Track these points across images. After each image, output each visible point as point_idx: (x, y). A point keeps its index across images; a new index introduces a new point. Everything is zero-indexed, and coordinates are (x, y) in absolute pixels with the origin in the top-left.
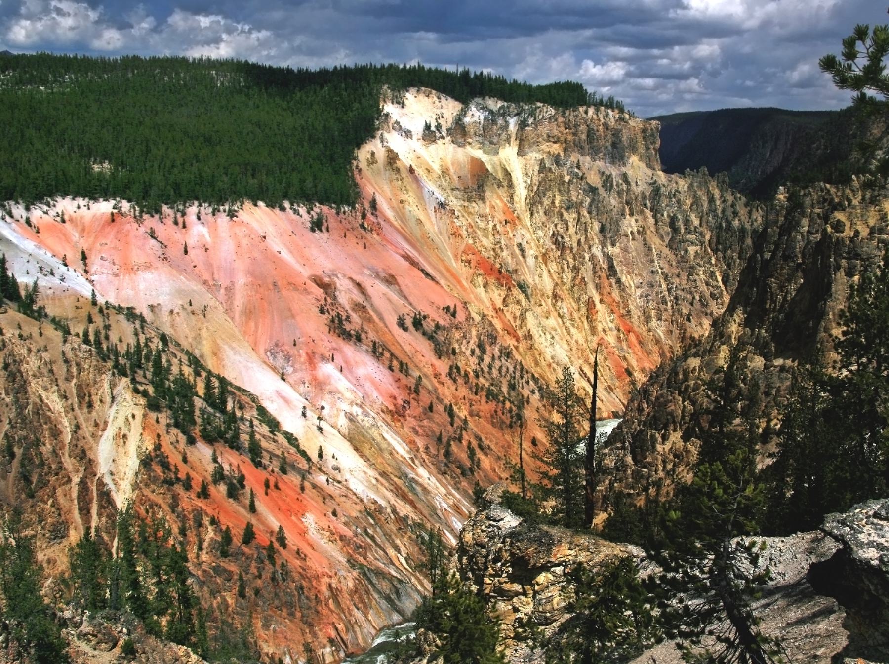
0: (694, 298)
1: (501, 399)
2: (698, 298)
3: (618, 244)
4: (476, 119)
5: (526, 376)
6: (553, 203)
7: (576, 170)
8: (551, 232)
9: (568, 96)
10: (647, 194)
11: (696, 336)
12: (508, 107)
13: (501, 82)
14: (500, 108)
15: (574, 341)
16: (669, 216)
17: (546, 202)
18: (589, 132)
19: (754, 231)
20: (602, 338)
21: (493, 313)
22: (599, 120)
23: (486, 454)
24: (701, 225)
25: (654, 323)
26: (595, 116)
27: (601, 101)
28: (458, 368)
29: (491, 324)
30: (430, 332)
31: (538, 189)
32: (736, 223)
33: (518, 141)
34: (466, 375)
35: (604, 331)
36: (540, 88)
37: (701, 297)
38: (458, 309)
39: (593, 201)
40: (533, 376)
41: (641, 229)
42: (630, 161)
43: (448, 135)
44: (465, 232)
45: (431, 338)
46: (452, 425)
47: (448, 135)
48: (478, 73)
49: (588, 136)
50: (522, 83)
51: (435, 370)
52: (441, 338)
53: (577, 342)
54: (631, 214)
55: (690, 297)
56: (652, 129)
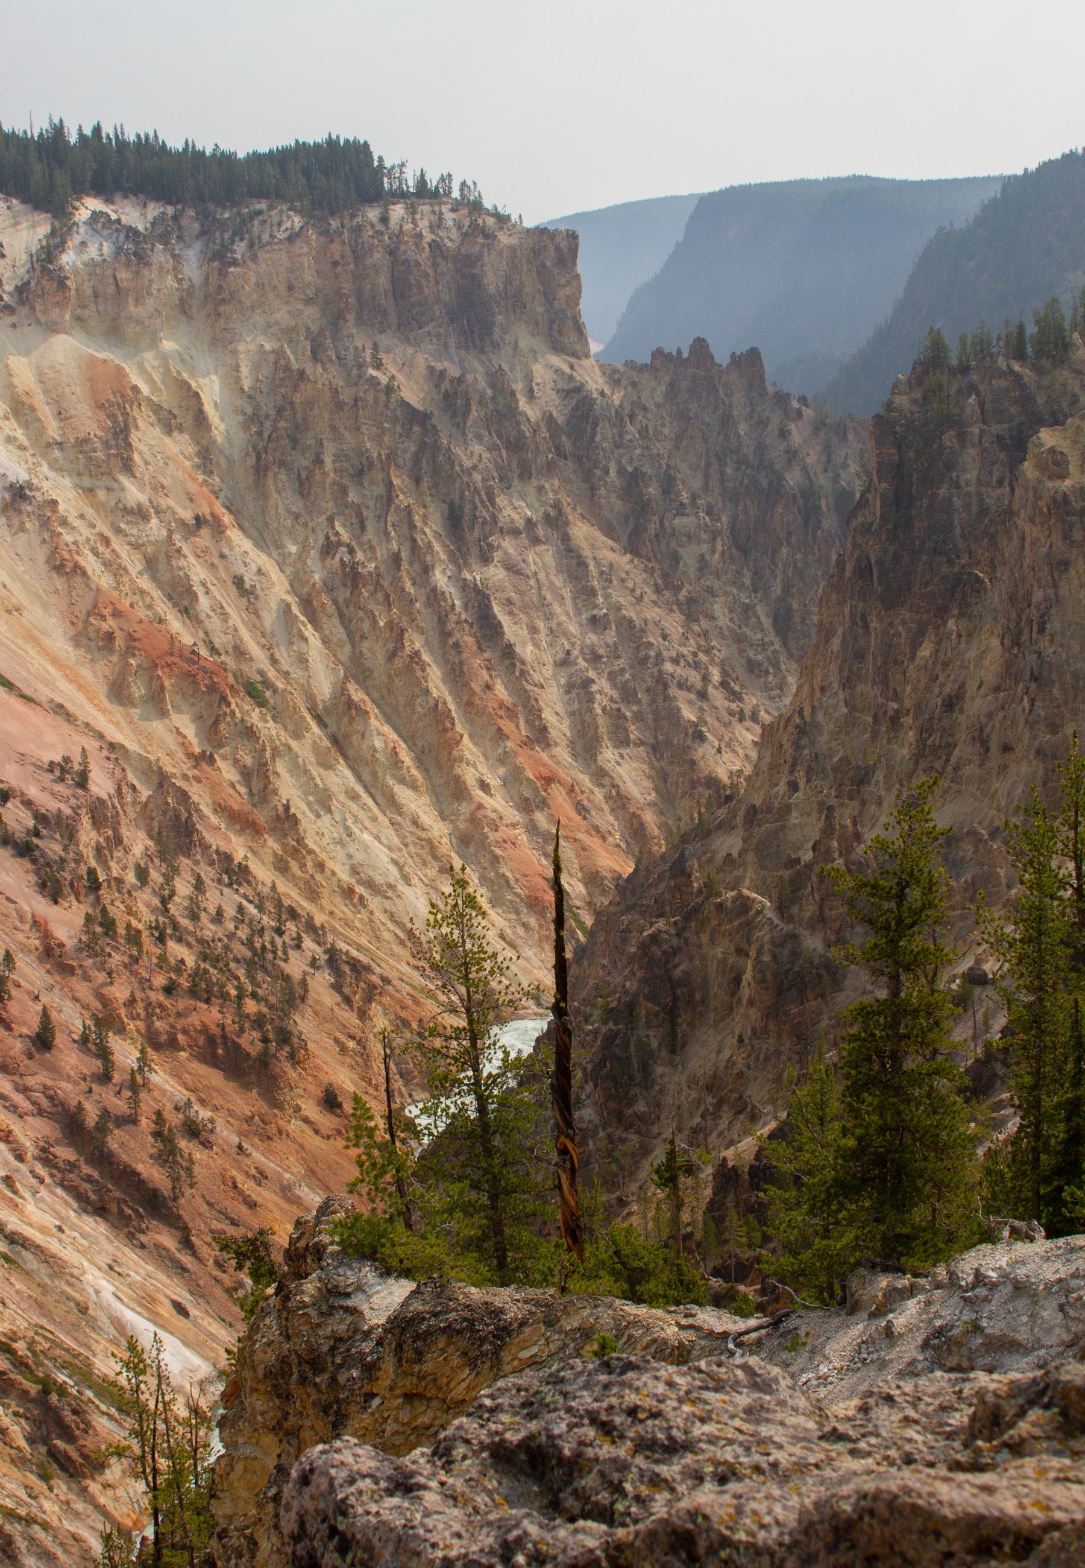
0: (706, 679)
1: (234, 992)
2: (716, 676)
3: (497, 556)
4: (93, 252)
5: (291, 927)
6: (319, 461)
7: (372, 372)
8: (321, 540)
9: (334, 177)
10: (561, 420)
11: (724, 777)
12: (175, 218)
13: (148, 150)
14: (153, 224)
15: (407, 824)
16: (622, 471)
17: (303, 461)
18: (393, 265)
19: (843, 495)
20: (480, 806)
21: (186, 767)
22: (420, 236)
23: (207, 1145)
24: (706, 487)
25: (608, 755)
26: (409, 227)
27: (422, 181)
28: (109, 925)
29: (184, 796)
30: (20, 836)
31: (275, 429)
32: (793, 479)
33: (209, 307)
34: (134, 937)
35: (484, 786)
36: (256, 158)
37: (724, 673)
38: (92, 766)
39: (422, 446)
40: (311, 927)
41: (552, 512)
42: (508, 338)
43: (22, 302)
44: (91, 558)
45: (24, 850)
46: (105, 1078)
47: (22, 302)
48: (88, 131)
49: (393, 280)
50: (208, 152)
51: (46, 935)
52: (52, 847)
53: (415, 822)
54: (525, 474)
55: (695, 678)
56: (558, 249)
